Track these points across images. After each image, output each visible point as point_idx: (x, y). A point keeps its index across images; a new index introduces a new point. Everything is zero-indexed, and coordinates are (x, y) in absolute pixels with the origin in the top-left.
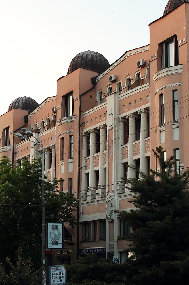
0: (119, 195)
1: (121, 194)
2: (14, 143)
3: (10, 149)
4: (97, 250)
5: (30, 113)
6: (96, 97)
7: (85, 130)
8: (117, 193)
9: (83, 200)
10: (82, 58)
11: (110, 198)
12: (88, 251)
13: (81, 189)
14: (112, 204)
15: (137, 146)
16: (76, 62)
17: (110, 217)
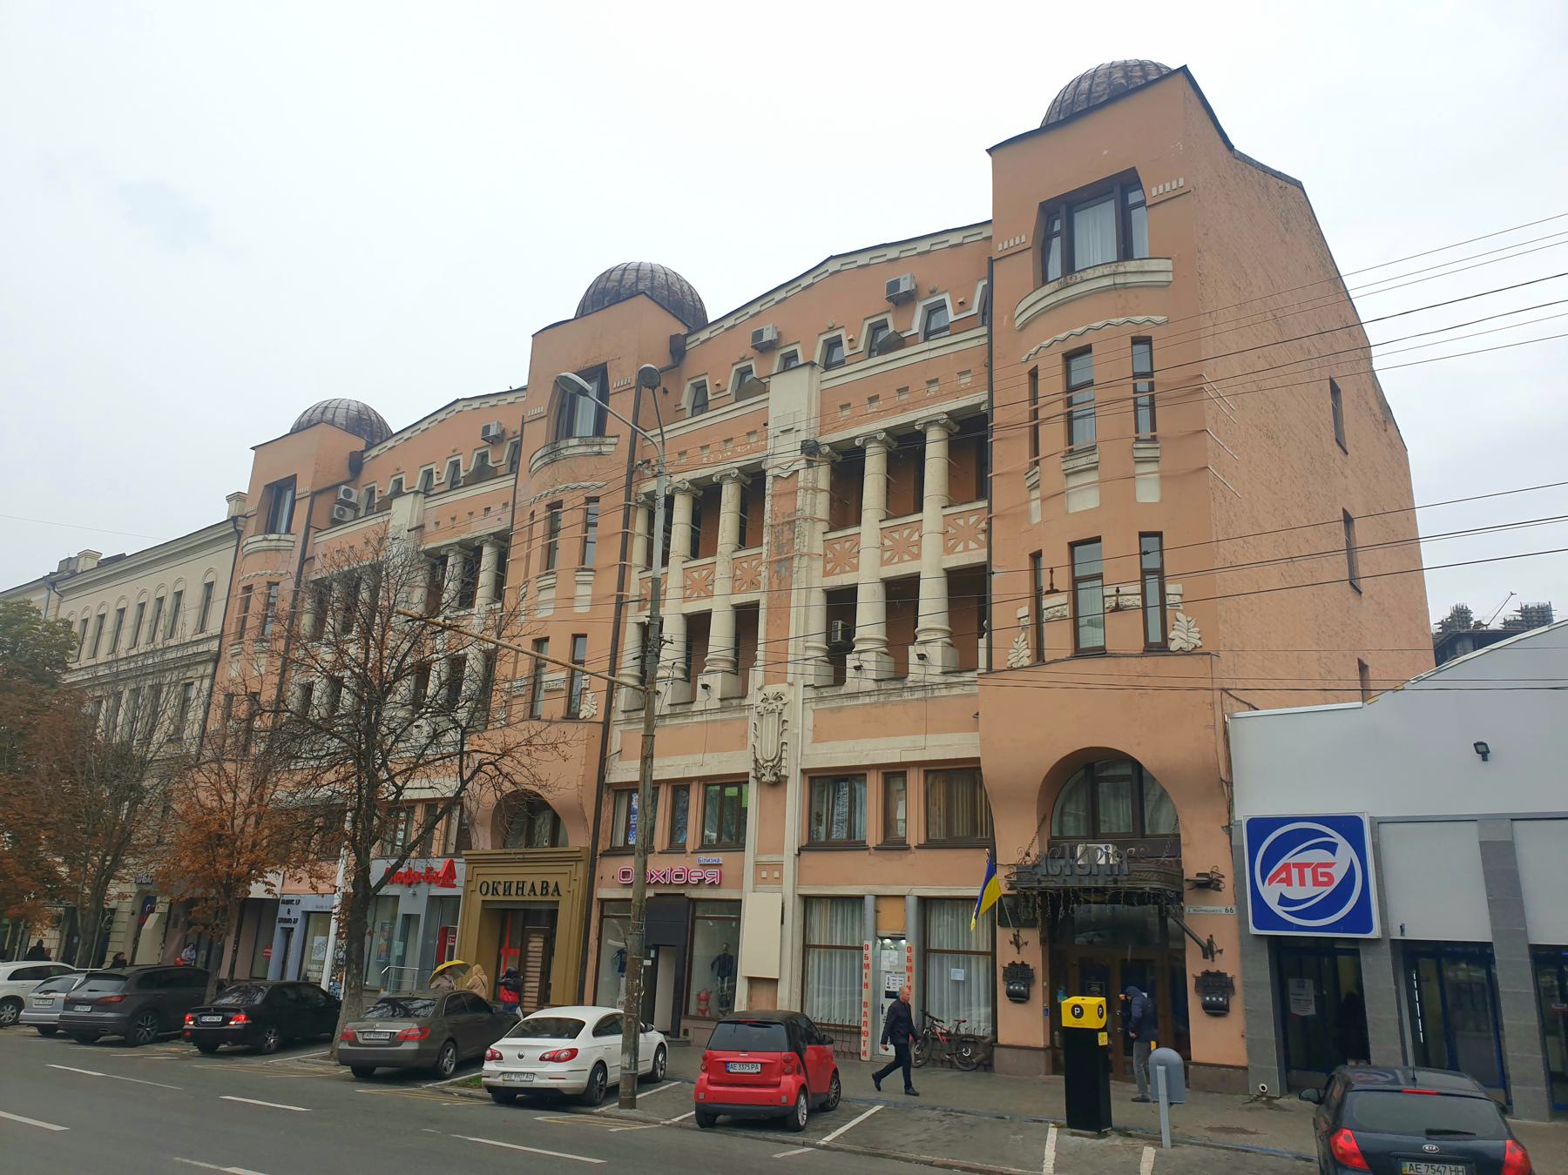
1: (822, 690)
3: (292, 544)
5: (369, 446)
6: (680, 395)
8: (805, 686)
9: (626, 709)
11: (775, 699)
14: (784, 721)
15: (901, 535)
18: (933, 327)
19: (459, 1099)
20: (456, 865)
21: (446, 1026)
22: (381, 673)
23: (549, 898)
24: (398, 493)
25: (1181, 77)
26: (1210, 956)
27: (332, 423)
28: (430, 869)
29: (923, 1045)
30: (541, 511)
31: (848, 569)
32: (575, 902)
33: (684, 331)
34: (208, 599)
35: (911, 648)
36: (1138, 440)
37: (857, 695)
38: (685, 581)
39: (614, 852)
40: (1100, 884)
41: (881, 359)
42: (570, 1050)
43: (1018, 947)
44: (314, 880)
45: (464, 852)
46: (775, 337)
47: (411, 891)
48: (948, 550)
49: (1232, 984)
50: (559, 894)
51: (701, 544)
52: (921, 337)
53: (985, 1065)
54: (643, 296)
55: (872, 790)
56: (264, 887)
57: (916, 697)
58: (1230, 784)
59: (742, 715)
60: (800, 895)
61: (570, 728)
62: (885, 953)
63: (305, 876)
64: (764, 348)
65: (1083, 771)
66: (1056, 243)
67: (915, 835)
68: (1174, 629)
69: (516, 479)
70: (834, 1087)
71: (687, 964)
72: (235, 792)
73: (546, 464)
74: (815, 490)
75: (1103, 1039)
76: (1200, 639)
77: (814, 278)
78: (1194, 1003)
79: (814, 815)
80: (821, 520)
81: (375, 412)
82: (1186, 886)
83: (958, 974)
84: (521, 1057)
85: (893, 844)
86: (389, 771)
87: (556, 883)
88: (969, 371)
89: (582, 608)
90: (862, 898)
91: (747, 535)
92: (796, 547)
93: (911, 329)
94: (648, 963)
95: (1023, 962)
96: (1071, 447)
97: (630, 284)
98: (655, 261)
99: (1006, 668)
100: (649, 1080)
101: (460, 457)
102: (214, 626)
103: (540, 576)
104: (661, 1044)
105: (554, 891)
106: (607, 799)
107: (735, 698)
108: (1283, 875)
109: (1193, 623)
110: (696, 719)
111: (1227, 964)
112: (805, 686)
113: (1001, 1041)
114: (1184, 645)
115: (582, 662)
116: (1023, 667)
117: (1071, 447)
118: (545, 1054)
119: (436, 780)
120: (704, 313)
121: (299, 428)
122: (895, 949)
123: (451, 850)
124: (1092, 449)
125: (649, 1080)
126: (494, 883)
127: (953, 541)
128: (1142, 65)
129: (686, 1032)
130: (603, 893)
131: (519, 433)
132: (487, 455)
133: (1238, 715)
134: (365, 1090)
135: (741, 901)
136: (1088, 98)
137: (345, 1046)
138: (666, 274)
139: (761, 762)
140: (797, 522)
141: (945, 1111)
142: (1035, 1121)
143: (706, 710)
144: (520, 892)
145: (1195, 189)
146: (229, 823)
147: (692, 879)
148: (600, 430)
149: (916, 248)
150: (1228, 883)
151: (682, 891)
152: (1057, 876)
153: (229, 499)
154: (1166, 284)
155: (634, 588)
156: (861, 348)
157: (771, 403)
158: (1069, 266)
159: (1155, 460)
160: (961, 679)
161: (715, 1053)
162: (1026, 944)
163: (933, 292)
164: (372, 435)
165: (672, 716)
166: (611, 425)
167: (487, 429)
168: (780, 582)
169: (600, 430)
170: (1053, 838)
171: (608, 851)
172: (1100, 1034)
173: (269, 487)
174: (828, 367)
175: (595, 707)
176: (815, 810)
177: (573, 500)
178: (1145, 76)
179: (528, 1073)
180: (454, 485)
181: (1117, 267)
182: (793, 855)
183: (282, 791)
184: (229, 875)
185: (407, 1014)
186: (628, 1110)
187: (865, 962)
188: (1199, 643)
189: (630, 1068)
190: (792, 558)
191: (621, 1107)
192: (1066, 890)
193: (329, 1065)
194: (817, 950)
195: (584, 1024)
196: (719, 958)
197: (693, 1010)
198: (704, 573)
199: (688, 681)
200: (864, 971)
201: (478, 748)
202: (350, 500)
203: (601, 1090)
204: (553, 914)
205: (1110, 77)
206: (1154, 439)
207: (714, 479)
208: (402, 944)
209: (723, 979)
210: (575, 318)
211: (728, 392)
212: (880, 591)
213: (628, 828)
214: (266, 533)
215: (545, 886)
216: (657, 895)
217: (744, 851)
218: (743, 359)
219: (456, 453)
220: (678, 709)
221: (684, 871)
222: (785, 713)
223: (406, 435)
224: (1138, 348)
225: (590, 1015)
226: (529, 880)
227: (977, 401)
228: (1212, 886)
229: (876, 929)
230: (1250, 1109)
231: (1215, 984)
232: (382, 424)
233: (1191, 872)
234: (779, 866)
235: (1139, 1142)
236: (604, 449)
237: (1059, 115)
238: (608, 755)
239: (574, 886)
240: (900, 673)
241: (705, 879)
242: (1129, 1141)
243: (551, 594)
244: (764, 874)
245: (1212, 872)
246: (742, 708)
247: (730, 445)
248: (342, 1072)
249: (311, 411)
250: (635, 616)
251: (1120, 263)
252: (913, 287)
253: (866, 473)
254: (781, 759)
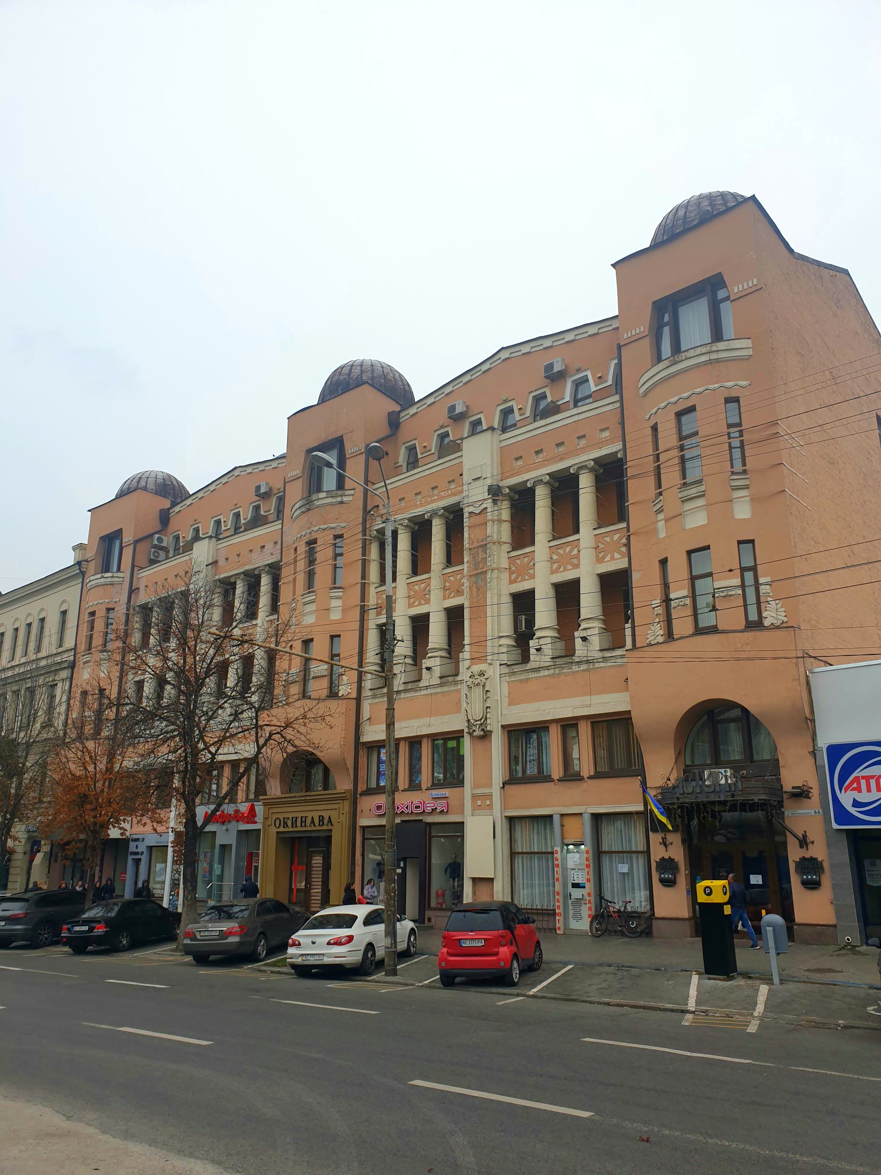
0: (509, 668)
1: (513, 667)
2: (133, 566)
3: (122, 580)
5: (174, 504)
6: (398, 457)
8: (500, 665)
9: (372, 688)
10: (361, 370)
13: (366, 661)
14: (487, 691)
15: (565, 551)
17: (481, 724)
18: (579, 396)
19: (272, 975)
20: (256, 807)
21: (259, 924)
22: (196, 672)
23: (325, 827)
24: (197, 538)
25: (751, 203)
26: (805, 848)
27: (145, 489)
28: (237, 811)
29: (601, 920)
30: (302, 549)
31: (527, 577)
32: (344, 829)
33: (398, 408)
34: (63, 623)
35: (576, 634)
36: (733, 473)
37: (538, 669)
38: (409, 593)
39: (369, 792)
40: (722, 798)
41: (543, 422)
42: (348, 936)
43: (666, 846)
44: (155, 824)
45: (261, 797)
46: (465, 409)
47: (224, 828)
48: (600, 560)
49: (822, 865)
50: (332, 824)
51: (419, 565)
52: (572, 404)
53: (647, 933)
54: (365, 387)
55: (554, 738)
56: (120, 831)
57: (582, 668)
58: (813, 721)
59: (456, 688)
60: (506, 817)
61: (333, 704)
62: (569, 855)
63: (148, 821)
64: (457, 418)
65: (706, 717)
66: (666, 330)
67: (586, 768)
68: (766, 610)
69: (282, 524)
70: (537, 953)
71: (427, 870)
72: (95, 764)
73: (303, 512)
74: (500, 521)
75: (727, 910)
76: (785, 616)
77: (491, 364)
78: (795, 880)
79: (513, 758)
80: (505, 543)
81: (176, 479)
82: (785, 796)
83: (624, 868)
84: (314, 943)
85: (571, 776)
86: (205, 743)
87: (330, 817)
88: (608, 428)
89: (335, 616)
90: (550, 817)
91: (452, 556)
92: (489, 564)
93: (564, 398)
94: (399, 871)
95: (670, 857)
96: (685, 481)
97: (356, 376)
98: (374, 358)
99: (646, 645)
100: (405, 955)
101: (240, 509)
102: (69, 643)
103: (304, 594)
104: (412, 929)
105: (328, 822)
106: (363, 754)
107: (450, 676)
108: (855, 785)
109: (780, 605)
110: (423, 693)
111: (818, 851)
112: (500, 665)
113: (657, 915)
114: (775, 622)
115: (338, 655)
116: (658, 643)
117: (685, 481)
118: (331, 940)
119: (239, 747)
120: (412, 393)
121: (122, 494)
122: (577, 852)
123: (252, 796)
124: (700, 482)
125: (405, 955)
126: (284, 818)
127: (602, 554)
128: (723, 195)
129: (429, 920)
130: (363, 822)
131: (282, 489)
132: (260, 507)
133: (816, 670)
134: (203, 971)
135: (463, 823)
136: (684, 222)
137: (187, 941)
138: (382, 367)
139: (472, 721)
140: (488, 545)
141: (618, 967)
142: (683, 971)
143: (430, 686)
144: (303, 825)
145: (765, 285)
146: (92, 786)
147: (427, 808)
148: (341, 483)
149: (564, 339)
150: (815, 793)
151: (421, 818)
152: (690, 794)
153: (75, 548)
154: (748, 357)
155: (372, 600)
156: (528, 414)
157: (464, 459)
158: (676, 348)
159: (747, 487)
160: (614, 654)
161: (452, 933)
162: (672, 843)
163: (579, 370)
164: (175, 496)
165: (406, 691)
166: (348, 484)
167: (258, 488)
168: (478, 590)
169: (341, 483)
170: (687, 766)
171: (365, 791)
172: (725, 907)
173: (102, 539)
174: (504, 429)
175: (350, 687)
176: (513, 755)
177: (325, 540)
178: (725, 202)
179: (319, 954)
180: (237, 530)
181: (711, 347)
182: (498, 788)
183: (129, 761)
184: (95, 824)
185: (230, 917)
186: (392, 977)
187: (556, 862)
188: (785, 619)
189: (392, 946)
190: (486, 572)
191: (386, 975)
192: (698, 804)
193: (176, 955)
194: (520, 856)
195: (356, 917)
196: (450, 864)
197: (433, 904)
198: (423, 585)
199: (416, 665)
200: (556, 869)
201: (268, 723)
202: (162, 545)
203: (372, 964)
204: (328, 840)
205: (699, 206)
206: (745, 472)
207: (426, 517)
208: (220, 866)
209: (454, 880)
210: (318, 404)
211: (433, 451)
212: (551, 593)
213: (379, 774)
214: (102, 572)
215: (321, 819)
216: (403, 821)
217: (464, 786)
218: (442, 427)
219: (237, 506)
220: (410, 686)
221: (421, 803)
222: (487, 685)
223: (200, 495)
224: (729, 405)
225: (361, 911)
226: (309, 815)
227: (614, 450)
228: (804, 795)
229: (563, 838)
230: (838, 955)
231: (810, 866)
232: (181, 487)
233: (788, 787)
234: (490, 796)
235: (758, 982)
236: (345, 499)
237: (663, 236)
238: (361, 722)
239: (343, 818)
240: (570, 652)
241: (436, 808)
242: (750, 982)
243: (311, 607)
244: (479, 803)
245: (803, 785)
246: (456, 683)
247: (436, 492)
248: (186, 960)
249: (129, 481)
250: (374, 620)
251: (713, 344)
252: (564, 367)
253: (536, 507)
254: (486, 719)
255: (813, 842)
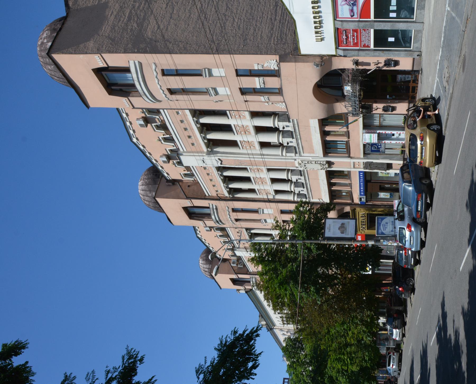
4: (361, 183)
7: (227, 194)
9: (305, 198)
12: (362, 193)
13: (293, 200)
14: (308, 163)
16: (150, 203)
17: (323, 165)
111: (382, 60)
112: (295, 156)
231: (388, 63)
236: (214, 208)
255: (378, 61)
